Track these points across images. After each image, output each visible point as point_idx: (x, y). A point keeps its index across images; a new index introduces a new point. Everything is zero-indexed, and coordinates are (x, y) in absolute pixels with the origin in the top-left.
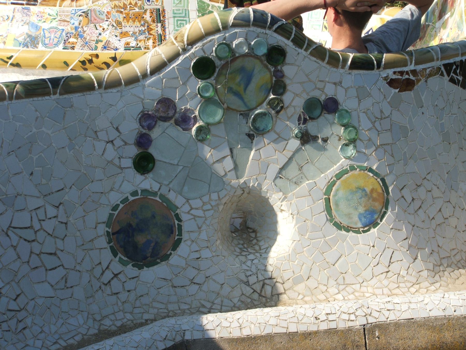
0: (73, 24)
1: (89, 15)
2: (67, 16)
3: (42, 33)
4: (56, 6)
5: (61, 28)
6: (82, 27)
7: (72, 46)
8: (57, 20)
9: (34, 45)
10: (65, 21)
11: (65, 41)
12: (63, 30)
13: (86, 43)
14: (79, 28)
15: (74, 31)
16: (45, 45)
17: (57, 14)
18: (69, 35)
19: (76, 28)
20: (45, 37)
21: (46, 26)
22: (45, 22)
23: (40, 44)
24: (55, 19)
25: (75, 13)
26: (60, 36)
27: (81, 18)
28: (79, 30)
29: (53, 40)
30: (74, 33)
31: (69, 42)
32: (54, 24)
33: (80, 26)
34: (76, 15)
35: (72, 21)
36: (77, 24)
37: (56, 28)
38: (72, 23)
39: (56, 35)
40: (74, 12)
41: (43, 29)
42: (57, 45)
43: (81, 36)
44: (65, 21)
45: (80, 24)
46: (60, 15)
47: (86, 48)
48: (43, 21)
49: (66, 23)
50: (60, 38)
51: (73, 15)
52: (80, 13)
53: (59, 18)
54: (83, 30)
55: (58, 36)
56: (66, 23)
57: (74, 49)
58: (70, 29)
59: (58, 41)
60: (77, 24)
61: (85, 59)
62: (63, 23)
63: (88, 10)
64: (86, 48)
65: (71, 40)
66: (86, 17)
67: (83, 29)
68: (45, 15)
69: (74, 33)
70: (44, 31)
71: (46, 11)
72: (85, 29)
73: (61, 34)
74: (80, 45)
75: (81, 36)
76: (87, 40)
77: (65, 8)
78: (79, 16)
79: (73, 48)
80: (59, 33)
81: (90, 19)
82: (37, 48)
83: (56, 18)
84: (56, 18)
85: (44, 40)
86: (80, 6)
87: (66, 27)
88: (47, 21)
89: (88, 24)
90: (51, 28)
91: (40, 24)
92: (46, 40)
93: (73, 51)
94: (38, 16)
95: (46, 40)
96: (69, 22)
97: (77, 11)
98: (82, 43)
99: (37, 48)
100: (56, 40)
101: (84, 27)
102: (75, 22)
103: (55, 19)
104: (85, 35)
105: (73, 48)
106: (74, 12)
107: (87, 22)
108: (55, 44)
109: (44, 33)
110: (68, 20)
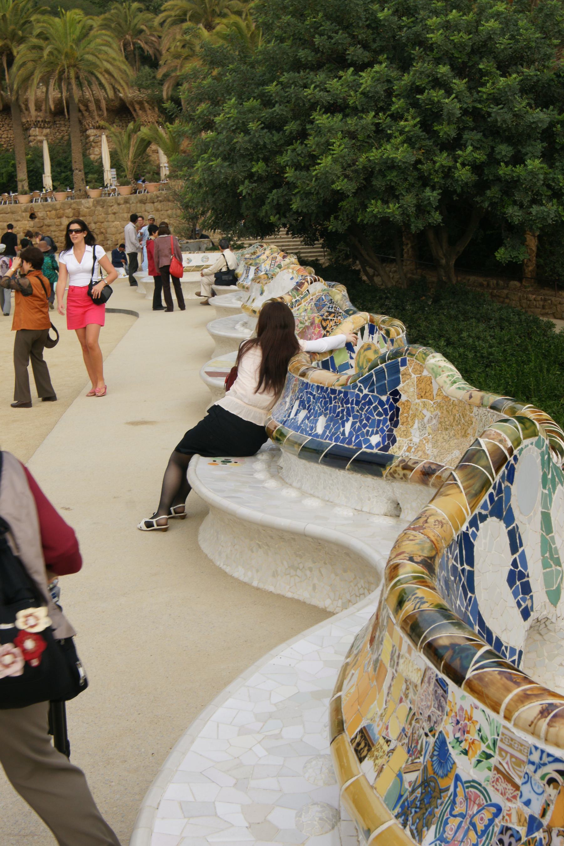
2: (519, 763)
5: (497, 798)
6: (549, 831)
10: (509, 779)
15: (523, 830)
26: (487, 827)
34: (540, 772)
41: (458, 778)
46: (501, 749)
51: (532, 768)
55: (480, 827)
73: (491, 821)
80: (487, 815)
87: (509, 804)
101: (554, 834)
102: (533, 797)
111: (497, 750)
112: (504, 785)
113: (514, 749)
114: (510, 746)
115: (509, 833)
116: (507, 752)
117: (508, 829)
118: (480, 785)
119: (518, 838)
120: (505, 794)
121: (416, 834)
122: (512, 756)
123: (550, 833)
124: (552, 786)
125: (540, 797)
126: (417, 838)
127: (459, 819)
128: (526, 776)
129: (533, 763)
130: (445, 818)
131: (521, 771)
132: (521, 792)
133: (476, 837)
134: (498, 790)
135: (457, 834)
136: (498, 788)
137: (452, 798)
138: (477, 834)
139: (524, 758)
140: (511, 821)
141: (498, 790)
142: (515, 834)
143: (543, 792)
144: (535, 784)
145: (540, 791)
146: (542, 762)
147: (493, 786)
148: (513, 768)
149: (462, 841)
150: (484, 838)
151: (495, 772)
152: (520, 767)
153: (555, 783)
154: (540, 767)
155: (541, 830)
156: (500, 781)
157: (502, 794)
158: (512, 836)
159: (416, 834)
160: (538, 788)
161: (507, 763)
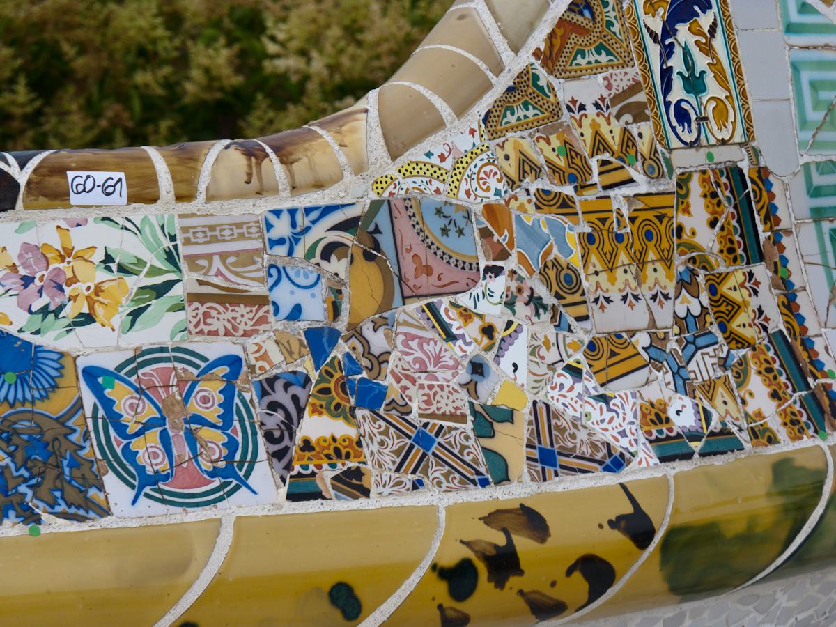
0: (295, 314)
1: (385, 240)
2: (247, 258)
3: (89, 400)
4: (154, 200)
5: (214, 349)
6: (356, 331)
7: (340, 468)
8: (178, 291)
9: (71, 494)
10: (233, 298)
11: (269, 436)
12: (234, 362)
13: (423, 440)
14: (334, 336)
15: (306, 365)
16: (145, 483)
17: (171, 257)
18: (281, 396)
19: (319, 341)
20: (121, 429)
21: (101, 345)
22: (87, 319)
23: (110, 480)
24: (161, 290)
25: (295, 239)
26: (227, 405)
27: (338, 266)
28: (340, 351)
29: (191, 438)
30: (314, 375)
31: (307, 445)
32: (160, 327)
33: (341, 325)
34: (300, 251)
35: (285, 296)
36: (315, 312)
37: (185, 355)
38: (285, 310)
39: (195, 407)
40: (282, 228)
41: (91, 374)
42: (232, 474)
43: (371, 397)
44: (233, 298)
45: (336, 311)
46: (192, 259)
47: (436, 472)
48: (70, 311)
49: (242, 309)
50: (227, 418)
52: (321, 233)
53: (188, 282)
54: (367, 352)
55: (213, 413)
56: (243, 313)
57: (366, 493)
58: (276, 355)
59: (231, 445)
60: (315, 312)
61: (467, 553)
62: (221, 318)
63: (375, 206)
64: (436, 472)
65: (315, 427)
66: (368, 257)
67: (366, 343)
68: (79, 266)
69: (314, 375)
70: (97, 390)
71: (79, 239)
72: (378, 342)
74: (388, 459)
75: (371, 397)
76: (414, 417)
77: (214, 206)
78: (326, 255)
79: (353, 483)
80: (212, 389)
81: (394, 269)
82: (105, 512)
83: (169, 285)
84: (169, 285)
85: (130, 455)
86: (319, 185)
87: (250, 343)
88: (99, 311)
89: (386, 305)
90: (142, 358)
91: (53, 339)
92: (136, 444)
93: (361, 504)
94: (27, 281)
95: (136, 444)
96: (261, 301)
97: (302, 221)
98: (395, 443)
99: (105, 512)
100: (213, 439)
101: (367, 331)
102: (302, 297)
103: (161, 290)
104: (388, 381)
105: (353, 483)
106: (282, 228)
107: (379, 293)
108: (214, 474)
109: (107, 403)
110: (258, 289)
111: (183, 265)
112: (229, 315)
113: (224, 241)
114: (214, 240)
115: (279, 385)
116: (209, 257)
117: (271, 382)
118: (162, 350)
119: (302, 382)
120: (235, 329)
121: (82, 512)
122: (224, 256)
123: (361, 335)
124: (333, 258)
125: (316, 290)
126: (92, 515)
127: (153, 435)
128: (274, 271)
129: (281, 241)
130: (119, 451)
131: (259, 270)
132: (274, 304)
133: (219, 432)
134: (216, 333)
135: (175, 453)
136: (213, 328)
137: (101, 413)
138: (214, 426)
139: (257, 244)
140: (272, 366)
141: (216, 333)
142: (292, 378)
143: (319, 276)
144: (298, 274)
145: (313, 278)
146: (298, 229)
147: (201, 332)
148: (237, 274)
149: (195, 457)
150: (236, 423)
151: (196, 304)
152: (254, 263)
153: (340, 249)
154: (297, 241)
155: (340, 341)
156: (213, 313)
157: (227, 334)
158: (286, 386)
159: (82, 512)
160: (306, 276)
161: (219, 273)
